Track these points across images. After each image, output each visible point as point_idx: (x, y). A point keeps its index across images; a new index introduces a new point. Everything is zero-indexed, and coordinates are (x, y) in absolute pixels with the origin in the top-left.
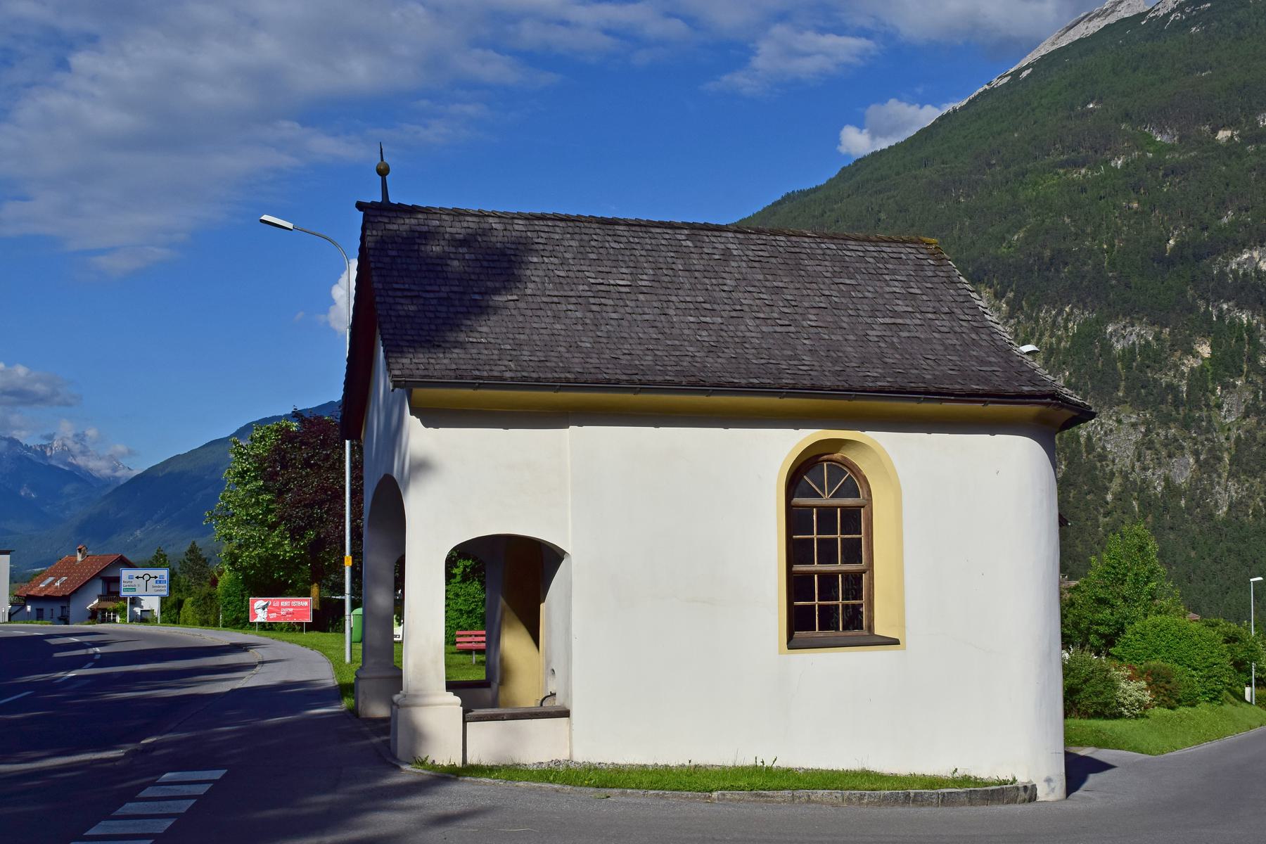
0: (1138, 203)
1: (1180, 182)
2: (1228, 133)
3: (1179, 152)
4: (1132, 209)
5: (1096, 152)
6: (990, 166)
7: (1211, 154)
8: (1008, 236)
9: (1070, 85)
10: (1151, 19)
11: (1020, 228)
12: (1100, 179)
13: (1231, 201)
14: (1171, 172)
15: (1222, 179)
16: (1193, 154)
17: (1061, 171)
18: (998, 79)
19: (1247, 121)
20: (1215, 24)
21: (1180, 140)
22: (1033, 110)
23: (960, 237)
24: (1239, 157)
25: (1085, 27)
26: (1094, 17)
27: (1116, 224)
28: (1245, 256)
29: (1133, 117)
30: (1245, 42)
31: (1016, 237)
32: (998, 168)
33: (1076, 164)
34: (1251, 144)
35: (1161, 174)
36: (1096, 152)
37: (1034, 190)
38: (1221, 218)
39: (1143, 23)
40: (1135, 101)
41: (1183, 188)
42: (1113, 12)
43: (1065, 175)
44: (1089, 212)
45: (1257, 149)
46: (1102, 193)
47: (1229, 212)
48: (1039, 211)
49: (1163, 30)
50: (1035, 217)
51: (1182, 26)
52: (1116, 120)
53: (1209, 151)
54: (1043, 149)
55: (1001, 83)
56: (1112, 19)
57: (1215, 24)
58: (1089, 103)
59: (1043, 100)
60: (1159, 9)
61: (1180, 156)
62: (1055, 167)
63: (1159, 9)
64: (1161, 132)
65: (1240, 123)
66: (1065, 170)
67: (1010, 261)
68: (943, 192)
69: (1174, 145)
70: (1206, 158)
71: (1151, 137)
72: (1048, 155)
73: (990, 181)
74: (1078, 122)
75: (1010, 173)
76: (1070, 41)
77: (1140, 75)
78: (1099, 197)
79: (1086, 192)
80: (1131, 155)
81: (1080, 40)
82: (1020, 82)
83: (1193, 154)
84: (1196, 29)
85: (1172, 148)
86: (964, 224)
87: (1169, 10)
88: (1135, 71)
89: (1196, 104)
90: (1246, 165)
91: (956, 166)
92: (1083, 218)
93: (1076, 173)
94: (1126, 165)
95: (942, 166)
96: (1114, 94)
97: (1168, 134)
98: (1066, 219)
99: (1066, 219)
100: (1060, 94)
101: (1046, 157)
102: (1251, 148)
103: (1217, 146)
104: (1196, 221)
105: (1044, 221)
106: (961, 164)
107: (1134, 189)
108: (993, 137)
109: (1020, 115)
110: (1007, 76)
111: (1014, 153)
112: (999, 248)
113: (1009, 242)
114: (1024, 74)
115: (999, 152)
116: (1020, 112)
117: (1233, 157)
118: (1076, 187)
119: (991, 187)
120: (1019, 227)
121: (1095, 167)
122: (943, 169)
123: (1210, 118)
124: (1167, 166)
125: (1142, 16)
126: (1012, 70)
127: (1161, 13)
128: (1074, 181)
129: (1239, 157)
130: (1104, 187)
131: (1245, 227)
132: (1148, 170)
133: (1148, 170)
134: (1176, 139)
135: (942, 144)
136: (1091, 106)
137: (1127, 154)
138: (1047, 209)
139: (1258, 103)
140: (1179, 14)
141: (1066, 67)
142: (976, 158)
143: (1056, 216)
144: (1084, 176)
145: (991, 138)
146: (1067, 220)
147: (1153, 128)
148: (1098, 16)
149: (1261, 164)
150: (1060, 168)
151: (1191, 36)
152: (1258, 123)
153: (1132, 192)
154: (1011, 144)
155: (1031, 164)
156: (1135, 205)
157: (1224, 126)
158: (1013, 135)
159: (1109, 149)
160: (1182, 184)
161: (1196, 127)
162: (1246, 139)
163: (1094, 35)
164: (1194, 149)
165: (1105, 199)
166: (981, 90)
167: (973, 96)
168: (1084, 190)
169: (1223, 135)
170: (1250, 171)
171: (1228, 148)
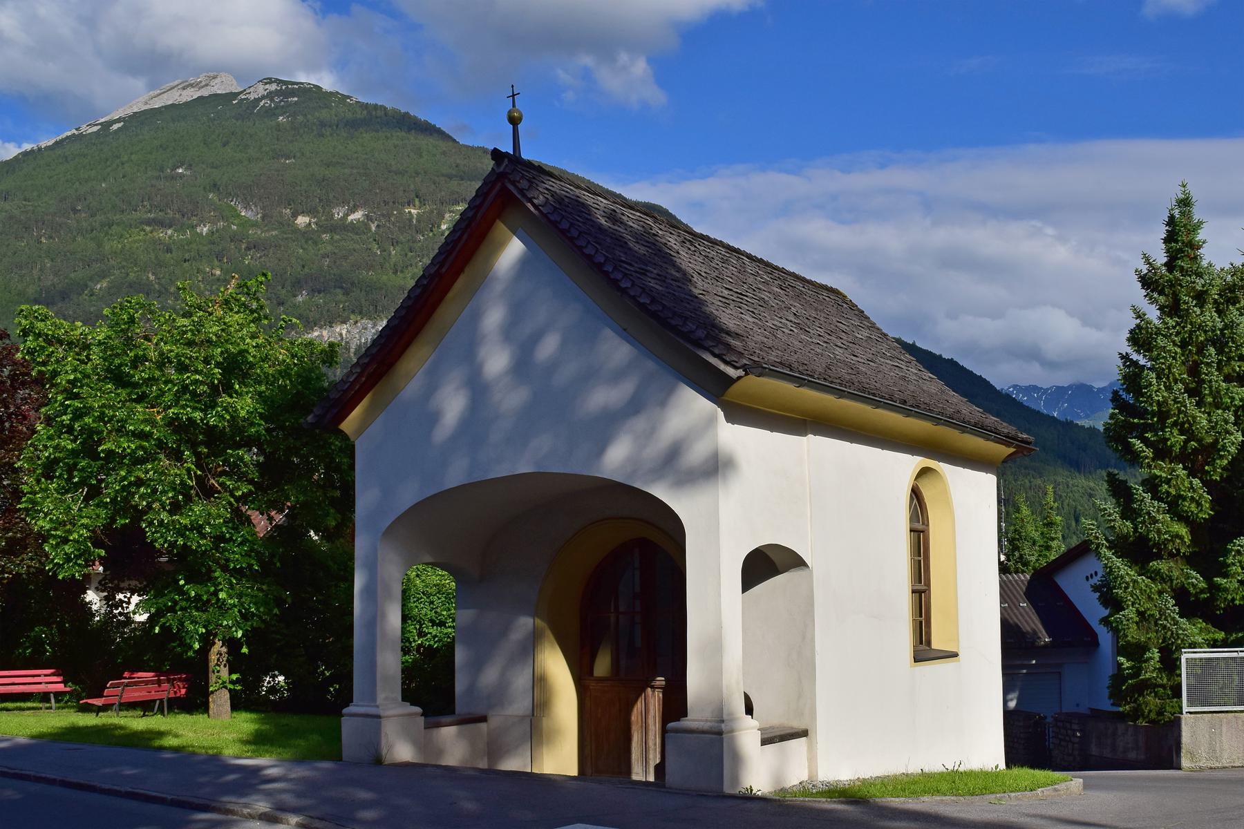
0: (221, 271)
1: (261, 257)
2: (307, 219)
3: (262, 229)
4: (215, 275)
5: (183, 216)
6: (75, 211)
7: (290, 236)
8: (90, 283)
9: (161, 146)
10: (242, 100)
11: (104, 278)
12: (185, 242)
13: (306, 282)
14: (253, 246)
15: (299, 260)
16: (274, 233)
17: (148, 229)
18: (87, 126)
19: (323, 212)
20: (300, 118)
21: (263, 218)
22: (123, 164)
23: (39, 278)
24: (315, 243)
25: (178, 94)
26: (188, 86)
27: (199, 288)
28: (316, 334)
29: (221, 189)
30: (326, 140)
31: (99, 286)
32: (83, 215)
33: (162, 224)
34: (325, 232)
35: (243, 247)
36: (183, 216)
37: (119, 242)
38: (295, 296)
39: (234, 102)
40: (223, 174)
41: (264, 263)
42: (207, 85)
43: (151, 233)
44: (174, 272)
45: (331, 238)
46: (187, 256)
47: (304, 292)
48: (124, 263)
49: (252, 113)
50: (119, 269)
51: (270, 113)
52: (204, 188)
53: (289, 233)
54: (130, 204)
55: (90, 131)
56: (205, 92)
57: (300, 118)
58: (178, 168)
59: (133, 156)
60: (250, 93)
61: (262, 233)
62: (142, 223)
63: (250, 93)
64: (246, 208)
65: (318, 212)
66: (151, 228)
67: (92, 309)
68: (24, 230)
69: (257, 221)
70: (286, 239)
71: (236, 211)
72: (136, 211)
73: (75, 226)
74: (167, 184)
75: (95, 221)
76: (163, 104)
77: (229, 150)
78: (183, 259)
79: (171, 253)
80: (217, 225)
81: (173, 105)
82: (111, 134)
83: (274, 233)
84: (283, 119)
85: (255, 225)
86: (45, 266)
87: (260, 95)
88: (224, 145)
89: (280, 187)
90: (321, 252)
91: (39, 206)
92: (167, 276)
93: (162, 232)
94: (211, 233)
95: (24, 203)
96: (203, 163)
97: (252, 210)
98: (150, 275)
99: (150, 275)
100: (151, 153)
101: (133, 213)
102: (326, 237)
103: (296, 230)
104: (273, 295)
105: (128, 275)
106: (44, 204)
107: (217, 257)
108: (80, 183)
109: (109, 166)
110: (97, 125)
111: (101, 203)
112: (81, 295)
113: (92, 290)
114: (115, 127)
115: (85, 199)
116: (108, 163)
117: (310, 242)
118: (162, 246)
119: (75, 233)
120: (103, 275)
121: (181, 229)
122: (25, 206)
123: (292, 203)
124: (249, 240)
125: (234, 95)
126: (102, 120)
127: (252, 97)
128: (160, 240)
129: (315, 243)
130: (189, 251)
131: (317, 307)
132: (232, 241)
133: (232, 241)
134: (259, 216)
135: (25, 181)
136: (180, 171)
137: (213, 223)
138: (131, 263)
139: (334, 196)
140: (269, 102)
141: (158, 128)
142: (61, 201)
143: (141, 271)
144: (170, 237)
145: (77, 183)
146: (152, 277)
147: (239, 203)
148: (191, 85)
149: (334, 253)
150: (146, 225)
151: (278, 124)
152: (333, 215)
153: (215, 259)
154: (98, 193)
155: (118, 217)
156: (218, 273)
157: (303, 212)
158: (101, 186)
159: (196, 215)
160: (263, 260)
161: (278, 209)
162: (323, 228)
163: (186, 104)
164: (276, 229)
165: (190, 262)
166: (69, 133)
167: (60, 138)
168: (169, 250)
169: (302, 220)
170: (325, 258)
171: (306, 233)
